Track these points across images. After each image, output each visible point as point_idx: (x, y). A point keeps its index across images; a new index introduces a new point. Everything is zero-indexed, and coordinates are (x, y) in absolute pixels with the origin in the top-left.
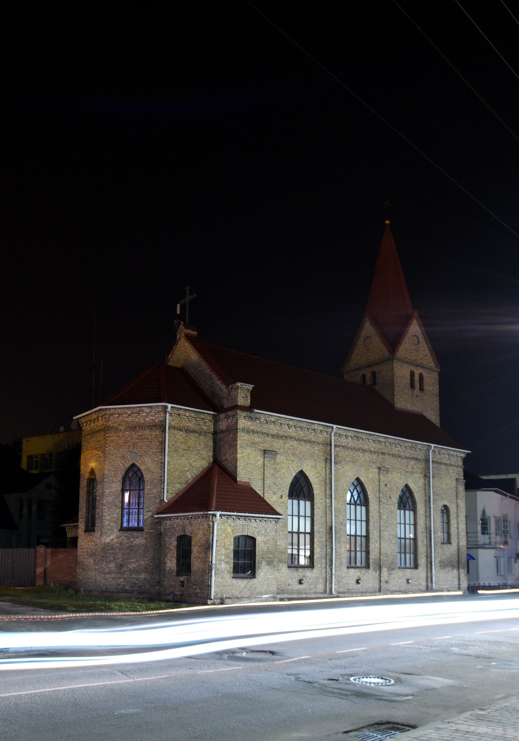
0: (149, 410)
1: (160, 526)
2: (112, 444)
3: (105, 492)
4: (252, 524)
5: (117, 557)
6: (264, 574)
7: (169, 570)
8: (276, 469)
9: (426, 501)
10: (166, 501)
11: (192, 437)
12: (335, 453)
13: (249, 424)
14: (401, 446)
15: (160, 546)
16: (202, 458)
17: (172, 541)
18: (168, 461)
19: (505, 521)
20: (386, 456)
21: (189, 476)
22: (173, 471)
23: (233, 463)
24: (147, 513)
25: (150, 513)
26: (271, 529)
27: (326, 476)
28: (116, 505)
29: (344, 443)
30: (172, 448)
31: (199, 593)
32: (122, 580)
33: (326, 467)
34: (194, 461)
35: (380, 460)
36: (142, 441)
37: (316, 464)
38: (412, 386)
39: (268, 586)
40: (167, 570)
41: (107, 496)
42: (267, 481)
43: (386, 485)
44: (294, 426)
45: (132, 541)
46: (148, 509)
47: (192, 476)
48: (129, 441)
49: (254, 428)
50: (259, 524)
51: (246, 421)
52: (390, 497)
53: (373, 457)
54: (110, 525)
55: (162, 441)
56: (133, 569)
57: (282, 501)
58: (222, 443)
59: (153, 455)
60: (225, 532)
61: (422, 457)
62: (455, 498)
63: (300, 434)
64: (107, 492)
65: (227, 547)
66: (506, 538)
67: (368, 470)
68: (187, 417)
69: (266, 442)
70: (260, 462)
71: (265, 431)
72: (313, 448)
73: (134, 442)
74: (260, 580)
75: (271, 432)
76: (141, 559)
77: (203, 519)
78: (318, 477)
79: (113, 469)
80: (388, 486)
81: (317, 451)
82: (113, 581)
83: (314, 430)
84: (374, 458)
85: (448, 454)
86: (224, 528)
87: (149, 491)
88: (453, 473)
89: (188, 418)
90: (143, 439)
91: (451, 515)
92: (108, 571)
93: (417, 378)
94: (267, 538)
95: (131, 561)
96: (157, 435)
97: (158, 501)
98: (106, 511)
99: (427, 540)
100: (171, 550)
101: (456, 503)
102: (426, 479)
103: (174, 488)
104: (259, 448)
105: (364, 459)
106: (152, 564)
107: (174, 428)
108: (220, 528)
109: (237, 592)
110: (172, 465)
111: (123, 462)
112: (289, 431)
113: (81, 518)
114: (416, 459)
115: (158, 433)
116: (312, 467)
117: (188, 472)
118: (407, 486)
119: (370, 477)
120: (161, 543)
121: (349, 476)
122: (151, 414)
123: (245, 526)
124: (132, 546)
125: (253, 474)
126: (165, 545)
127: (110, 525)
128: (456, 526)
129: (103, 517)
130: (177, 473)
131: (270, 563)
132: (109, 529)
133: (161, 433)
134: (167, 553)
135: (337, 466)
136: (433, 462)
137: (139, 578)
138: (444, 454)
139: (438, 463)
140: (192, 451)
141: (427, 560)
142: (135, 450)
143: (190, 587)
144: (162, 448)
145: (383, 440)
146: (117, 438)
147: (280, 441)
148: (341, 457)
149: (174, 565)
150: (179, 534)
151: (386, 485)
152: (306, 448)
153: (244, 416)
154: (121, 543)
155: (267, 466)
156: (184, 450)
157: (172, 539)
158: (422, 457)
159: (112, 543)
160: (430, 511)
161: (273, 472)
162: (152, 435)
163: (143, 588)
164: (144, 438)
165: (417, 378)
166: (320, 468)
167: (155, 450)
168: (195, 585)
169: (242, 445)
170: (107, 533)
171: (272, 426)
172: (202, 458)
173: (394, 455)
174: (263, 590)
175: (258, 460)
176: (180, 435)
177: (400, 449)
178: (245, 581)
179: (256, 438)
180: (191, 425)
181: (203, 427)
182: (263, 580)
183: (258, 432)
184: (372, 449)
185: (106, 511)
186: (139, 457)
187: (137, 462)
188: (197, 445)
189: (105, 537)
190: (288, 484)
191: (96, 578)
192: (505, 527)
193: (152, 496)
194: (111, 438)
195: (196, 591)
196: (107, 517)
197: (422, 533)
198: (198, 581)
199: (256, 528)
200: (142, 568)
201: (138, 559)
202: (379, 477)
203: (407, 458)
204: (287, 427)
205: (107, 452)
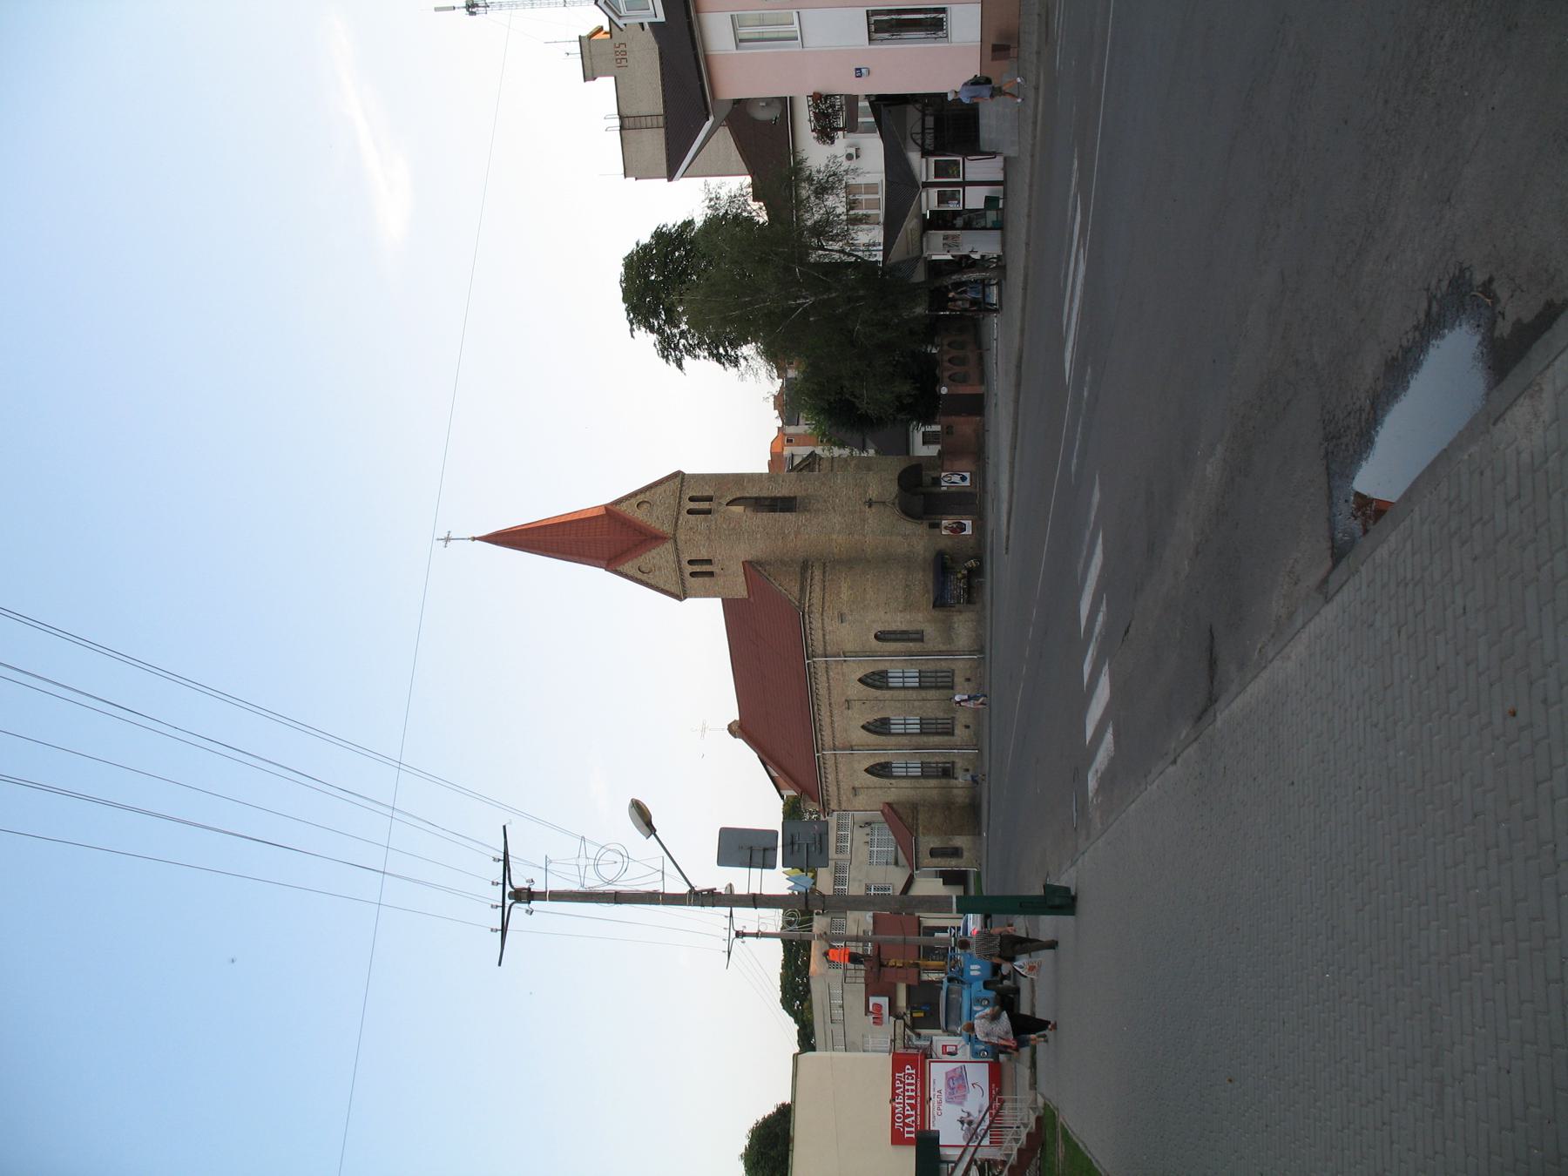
20: (832, 701)
75: (835, 789)
83: (824, 763)
93: (697, 568)
114: (827, 671)
118: (860, 680)
139: (825, 646)
145: (816, 708)
165: (697, 568)
171: (830, 789)
183: (839, 797)
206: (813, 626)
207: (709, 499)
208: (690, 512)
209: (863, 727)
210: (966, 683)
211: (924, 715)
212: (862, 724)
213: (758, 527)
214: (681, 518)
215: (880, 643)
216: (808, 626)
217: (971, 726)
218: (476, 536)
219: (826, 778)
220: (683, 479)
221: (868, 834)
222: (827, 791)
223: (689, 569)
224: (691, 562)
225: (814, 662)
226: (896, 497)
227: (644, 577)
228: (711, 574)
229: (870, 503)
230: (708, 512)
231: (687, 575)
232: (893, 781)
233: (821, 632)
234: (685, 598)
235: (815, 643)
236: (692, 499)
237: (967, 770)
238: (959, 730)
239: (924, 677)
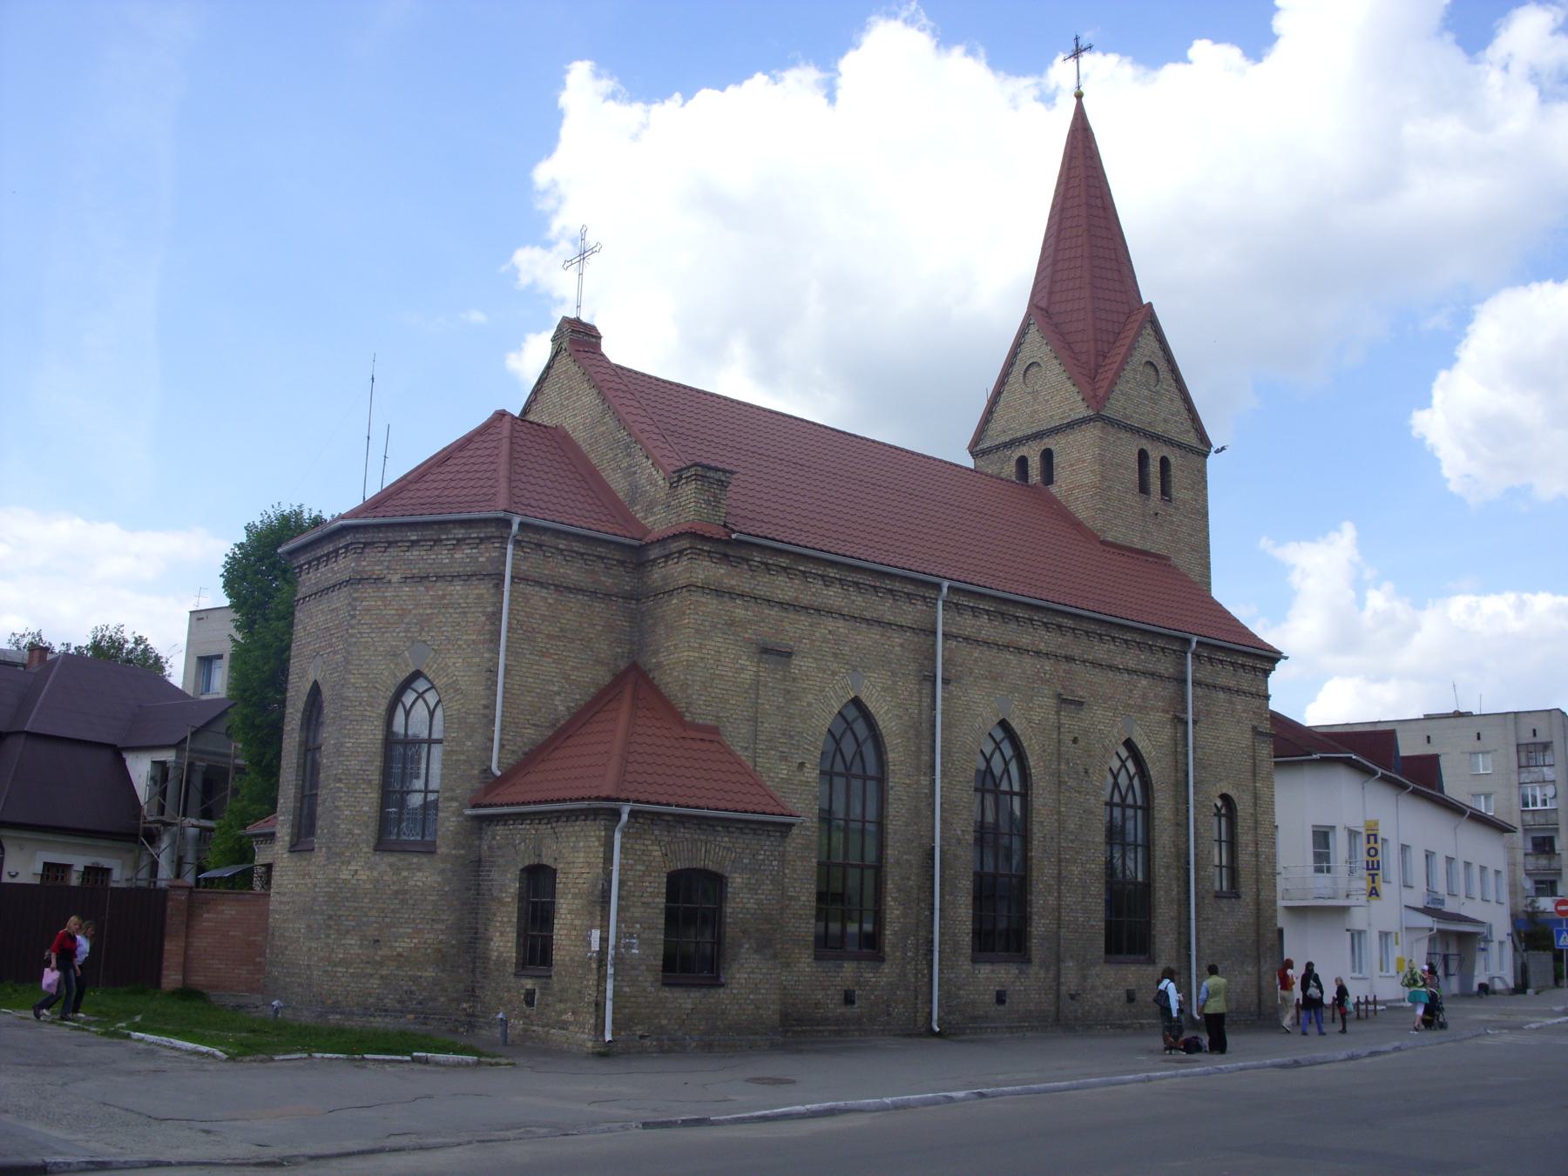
0: (463, 531)
1: (480, 839)
2: (368, 617)
3: (342, 744)
4: (719, 839)
5: (365, 919)
6: (746, 976)
7: (498, 957)
8: (789, 692)
9: (1176, 784)
10: (499, 773)
11: (571, 605)
12: (946, 653)
13: (722, 571)
14: (1113, 638)
15: (478, 894)
16: (596, 661)
17: (507, 881)
18: (506, 665)
19: (1372, 838)
20: (1077, 668)
21: (561, 708)
22: (518, 692)
23: (676, 674)
24: (449, 804)
25: (455, 804)
26: (768, 853)
27: (920, 713)
28: (370, 781)
30: (521, 632)
31: (571, 1023)
32: (377, 982)
33: (919, 691)
34: (574, 668)
35: (1061, 674)
36: (443, 610)
37: (895, 683)
38: (1144, 488)
39: (757, 1008)
40: (494, 958)
41: (347, 756)
42: (766, 725)
43: (1075, 741)
44: (840, 580)
45: (405, 878)
46: (447, 795)
47: (568, 708)
48: (410, 611)
49: (733, 582)
50: (737, 838)
51: (713, 565)
52: (1086, 772)
53: (1042, 667)
54: (350, 832)
55: (494, 614)
56: (405, 954)
57: (803, 778)
58: (650, 622)
59: (469, 650)
60: (645, 858)
61: (1166, 669)
62: (1249, 775)
63: (853, 601)
64: (347, 745)
65: (650, 900)
66: (1373, 882)
67: (1031, 700)
68: (562, 550)
69: (763, 622)
70: (747, 676)
71: (762, 591)
72: (889, 638)
73: (421, 615)
74: (735, 991)
76: (429, 927)
77: (588, 823)
79: (365, 685)
80: (1082, 743)
81: (898, 649)
82: (353, 985)
83: (891, 591)
84: (1047, 668)
85: (1232, 664)
86: (642, 848)
87: (454, 744)
88: (1244, 711)
89: (565, 553)
90: (446, 606)
91: (1240, 822)
92: (341, 956)
94: (756, 877)
95: (402, 930)
96: (480, 597)
97: (476, 772)
98: (342, 794)
99: (1178, 887)
100: (504, 904)
101: (1251, 788)
102: (1178, 727)
103: (519, 739)
104: (747, 636)
105: (1019, 671)
106: (454, 942)
107: (525, 579)
108: (632, 848)
109: (673, 1021)
110: (518, 678)
111: (392, 666)
112: (825, 592)
113: (283, 814)
115: (485, 591)
116: (884, 689)
117: (558, 698)
119: (1036, 719)
120: (479, 885)
121: (981, 715)
122: (467, 542)
123: (699, 844)
124: (405, 892)
125: (728, 706)
126: (490, 890)
127: (350, 832)
128: (1251, 849)
129: (336, 812)
130: (530, 699)
131: (764, 945)
132: (349, 843)
133: (492, 591)
134: (495, 915)
135: (950, 687)
136: (1196, 683)
137: (420, 977)
138: (1221, 661)
140: (572, 641)
141: (1179, 940)
142: (425, 637)
143: (547, 1005)
144: (491, 632)
146: (379, 603)
147: (802, 618)
148: (961, 666)
149: (510, 945)
150: (527, 864)
151: (1075, 741)
152: (868, 638)
153: (709, 552)
154: (378, 881)
155: (765, 686)
156: (550, 637)
157: (509, 875)
158: (1166, 669)
159: (354, 882)
160: (1188, 811)
161: (781, 700)
162: (467, 597)
163: (430, 1004)
164: (448, 604)
166: (905, 693)
167: (474, 637)
168: (560, 1001)
169: (702, 628)
170: (343, 853)
171: (781, 579)
172: (596, 661)
173: (1096, 664)
174: (744, 1017)
175: (743, 669)
176: (541, 599)
177: (1112, 647)
178: (696, 994)
179: (737, 611)
180: (569, 572)
181: (603, 579)
182: (743, 991)
184: (1042, 646)
185: (342, 794)
186: (432, 655)
187: (427, 665)
188: (586, 625)
189: (338, 864)
190: (820, 734)
191: (312, 974)
192: (1372, 852)
193: (463, 757)
194: (364, 603)
195: (564, 1017)
196: (346, 813)
197: (1168, 867)
198: (570, 991)
199: (728, 849)
200: (429, 951)
201: (420, 926)
202: (1059, 719)
203: (1128, 671)
204: (820, 582)
205: (354, 640)
210: (1121, 992)
216: (1249, 662)
217: (1001, 1008)
218: (1084, 100)
227: (1162, 366)
237: (849, 999)
238: (994, 975)
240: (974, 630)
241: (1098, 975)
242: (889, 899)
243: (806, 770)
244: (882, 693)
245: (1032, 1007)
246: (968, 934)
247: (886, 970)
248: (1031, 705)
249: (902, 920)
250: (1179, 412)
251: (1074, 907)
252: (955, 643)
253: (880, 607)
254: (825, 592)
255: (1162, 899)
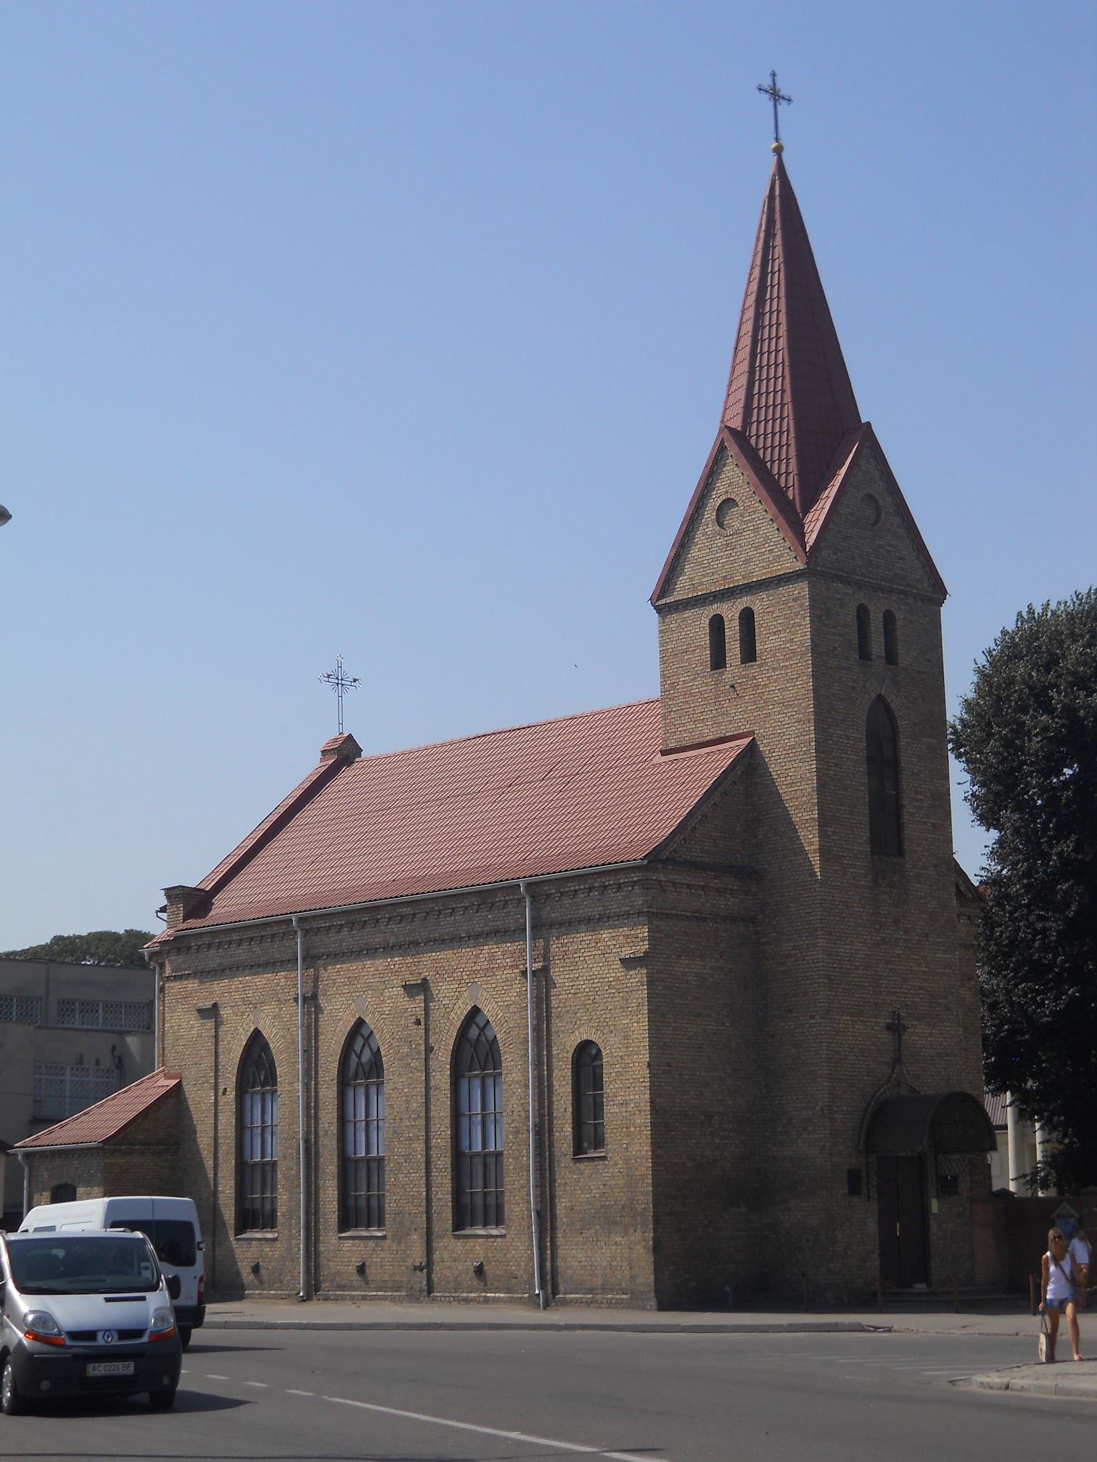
13: (181, 960)
29: (333, 946)
43: (418, 1022)
63: (254, 952)
78: (284, 1037)
83: (273, 936)
105: (372, 969)
112: (237, 952)
116: (274, 1017)
125: (186, 1057)
165: (732, 631)
206: (610, 893)
207: (891, 658)
208: (862, 614)
209: (360, 1023)
211: (389, 1166)
212: (367, 1020)
213: (836, 765)
214: (849, 590)
215: (570, 1055)
219: (240, 942)
220: (930, 600)
221: (98, 1062)
222: (209, 946)
223: (730, 612)
224: (747, 617)
225: (520, 901)
226: (912, 1089)
228: (718, 661)
229: (896, 1029)
230: (864, 654)
231: (715, 609)
232: (231, 1095)
233: (596, 911)
234: (659, 609)
235: (567, 901)
236: (889, 619)
239: (485, 1166)
240: (337, 945)
241: (446, 1247)
242: (279, 1186)
243: (227, 1093)
244: (272, 1021)
245: (386, 1277)
246: (334, 1212)
247: (278, 1245)
248: (382, 999)
249: (288, 1204)
250: (767, 539)
251: (417, 1182)
252: (322, 962)
253: (271, 950)
254: (237, 952)
255: (511, 1167)
